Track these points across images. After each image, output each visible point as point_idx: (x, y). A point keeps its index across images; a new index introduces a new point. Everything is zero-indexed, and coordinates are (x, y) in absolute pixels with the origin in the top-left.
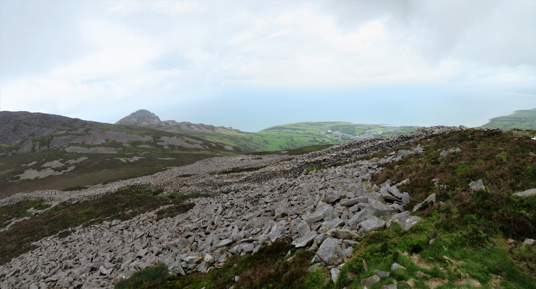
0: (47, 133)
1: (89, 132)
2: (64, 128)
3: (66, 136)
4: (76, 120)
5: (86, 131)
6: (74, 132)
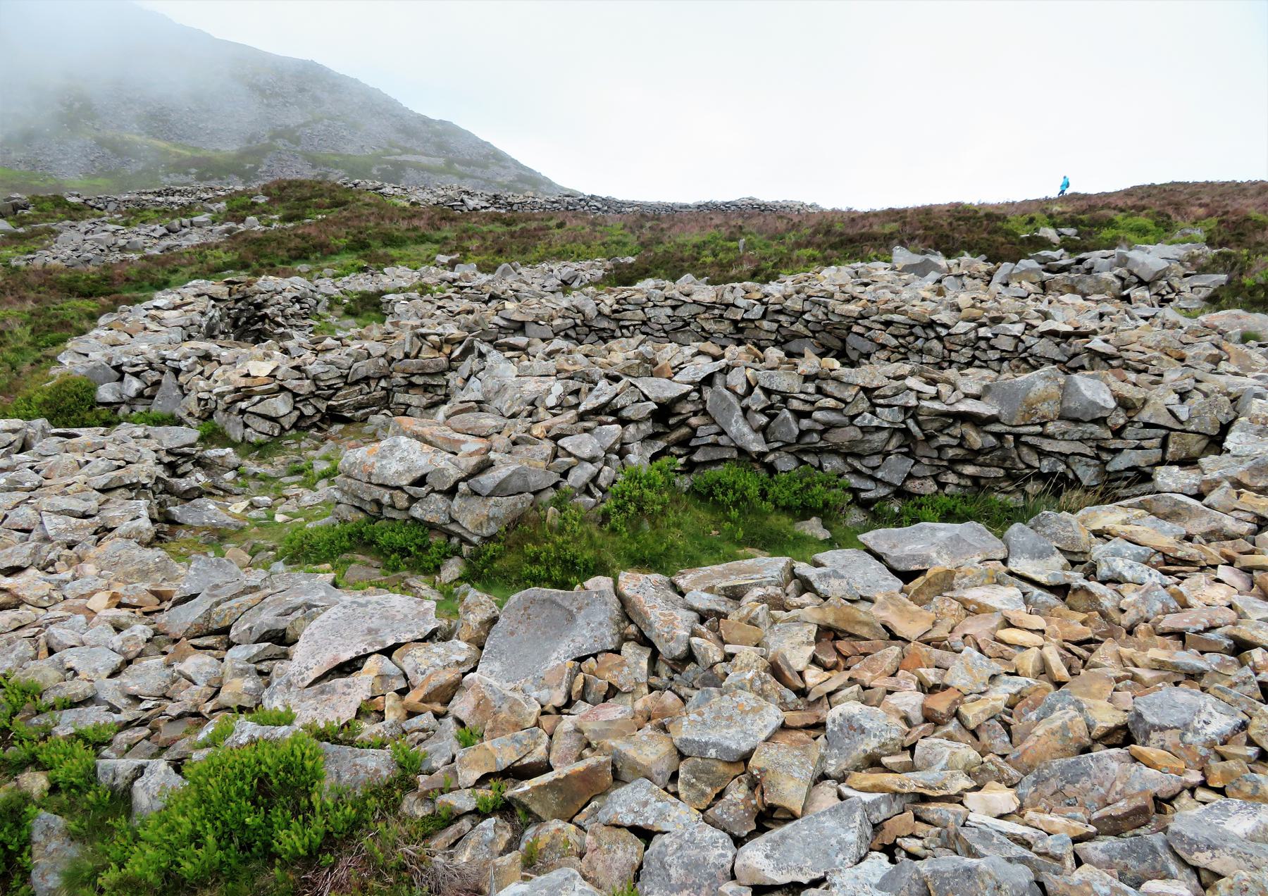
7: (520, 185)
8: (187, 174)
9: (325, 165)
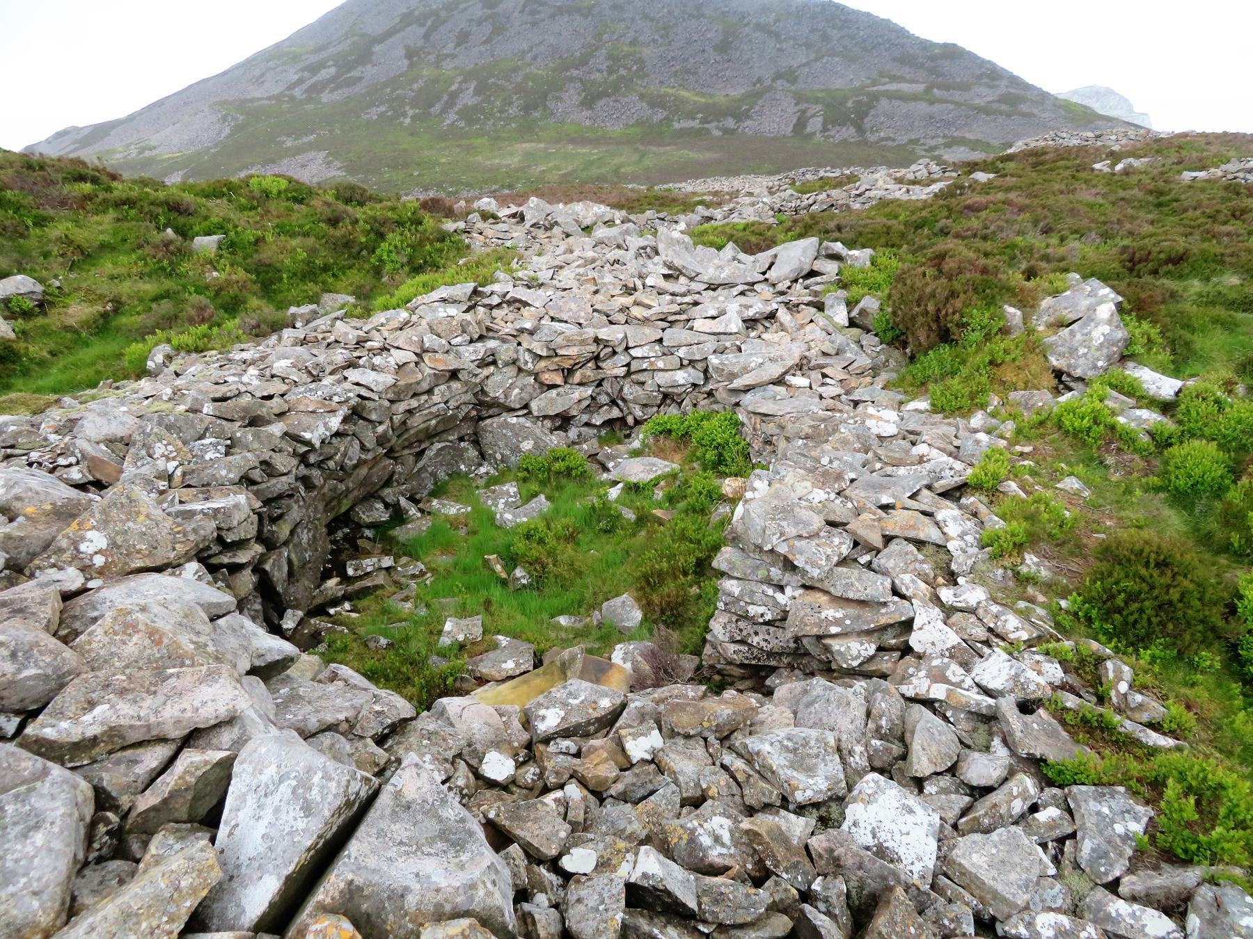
0: (844, 79)
1: (1024, 108)
2: (906, 71)
3: (932, 103)
4: (952, 53)
5: (1003, 99)
6: (957, 95)
7: (995, 106)
8: (694, 119)
9: (807, 101)
